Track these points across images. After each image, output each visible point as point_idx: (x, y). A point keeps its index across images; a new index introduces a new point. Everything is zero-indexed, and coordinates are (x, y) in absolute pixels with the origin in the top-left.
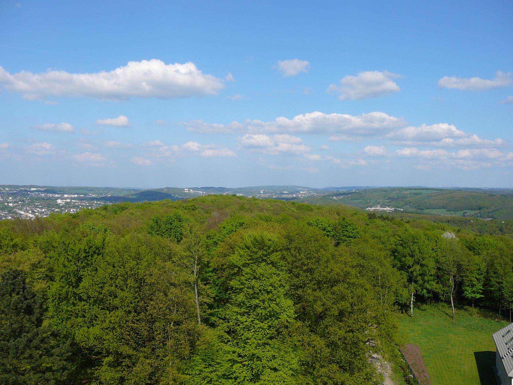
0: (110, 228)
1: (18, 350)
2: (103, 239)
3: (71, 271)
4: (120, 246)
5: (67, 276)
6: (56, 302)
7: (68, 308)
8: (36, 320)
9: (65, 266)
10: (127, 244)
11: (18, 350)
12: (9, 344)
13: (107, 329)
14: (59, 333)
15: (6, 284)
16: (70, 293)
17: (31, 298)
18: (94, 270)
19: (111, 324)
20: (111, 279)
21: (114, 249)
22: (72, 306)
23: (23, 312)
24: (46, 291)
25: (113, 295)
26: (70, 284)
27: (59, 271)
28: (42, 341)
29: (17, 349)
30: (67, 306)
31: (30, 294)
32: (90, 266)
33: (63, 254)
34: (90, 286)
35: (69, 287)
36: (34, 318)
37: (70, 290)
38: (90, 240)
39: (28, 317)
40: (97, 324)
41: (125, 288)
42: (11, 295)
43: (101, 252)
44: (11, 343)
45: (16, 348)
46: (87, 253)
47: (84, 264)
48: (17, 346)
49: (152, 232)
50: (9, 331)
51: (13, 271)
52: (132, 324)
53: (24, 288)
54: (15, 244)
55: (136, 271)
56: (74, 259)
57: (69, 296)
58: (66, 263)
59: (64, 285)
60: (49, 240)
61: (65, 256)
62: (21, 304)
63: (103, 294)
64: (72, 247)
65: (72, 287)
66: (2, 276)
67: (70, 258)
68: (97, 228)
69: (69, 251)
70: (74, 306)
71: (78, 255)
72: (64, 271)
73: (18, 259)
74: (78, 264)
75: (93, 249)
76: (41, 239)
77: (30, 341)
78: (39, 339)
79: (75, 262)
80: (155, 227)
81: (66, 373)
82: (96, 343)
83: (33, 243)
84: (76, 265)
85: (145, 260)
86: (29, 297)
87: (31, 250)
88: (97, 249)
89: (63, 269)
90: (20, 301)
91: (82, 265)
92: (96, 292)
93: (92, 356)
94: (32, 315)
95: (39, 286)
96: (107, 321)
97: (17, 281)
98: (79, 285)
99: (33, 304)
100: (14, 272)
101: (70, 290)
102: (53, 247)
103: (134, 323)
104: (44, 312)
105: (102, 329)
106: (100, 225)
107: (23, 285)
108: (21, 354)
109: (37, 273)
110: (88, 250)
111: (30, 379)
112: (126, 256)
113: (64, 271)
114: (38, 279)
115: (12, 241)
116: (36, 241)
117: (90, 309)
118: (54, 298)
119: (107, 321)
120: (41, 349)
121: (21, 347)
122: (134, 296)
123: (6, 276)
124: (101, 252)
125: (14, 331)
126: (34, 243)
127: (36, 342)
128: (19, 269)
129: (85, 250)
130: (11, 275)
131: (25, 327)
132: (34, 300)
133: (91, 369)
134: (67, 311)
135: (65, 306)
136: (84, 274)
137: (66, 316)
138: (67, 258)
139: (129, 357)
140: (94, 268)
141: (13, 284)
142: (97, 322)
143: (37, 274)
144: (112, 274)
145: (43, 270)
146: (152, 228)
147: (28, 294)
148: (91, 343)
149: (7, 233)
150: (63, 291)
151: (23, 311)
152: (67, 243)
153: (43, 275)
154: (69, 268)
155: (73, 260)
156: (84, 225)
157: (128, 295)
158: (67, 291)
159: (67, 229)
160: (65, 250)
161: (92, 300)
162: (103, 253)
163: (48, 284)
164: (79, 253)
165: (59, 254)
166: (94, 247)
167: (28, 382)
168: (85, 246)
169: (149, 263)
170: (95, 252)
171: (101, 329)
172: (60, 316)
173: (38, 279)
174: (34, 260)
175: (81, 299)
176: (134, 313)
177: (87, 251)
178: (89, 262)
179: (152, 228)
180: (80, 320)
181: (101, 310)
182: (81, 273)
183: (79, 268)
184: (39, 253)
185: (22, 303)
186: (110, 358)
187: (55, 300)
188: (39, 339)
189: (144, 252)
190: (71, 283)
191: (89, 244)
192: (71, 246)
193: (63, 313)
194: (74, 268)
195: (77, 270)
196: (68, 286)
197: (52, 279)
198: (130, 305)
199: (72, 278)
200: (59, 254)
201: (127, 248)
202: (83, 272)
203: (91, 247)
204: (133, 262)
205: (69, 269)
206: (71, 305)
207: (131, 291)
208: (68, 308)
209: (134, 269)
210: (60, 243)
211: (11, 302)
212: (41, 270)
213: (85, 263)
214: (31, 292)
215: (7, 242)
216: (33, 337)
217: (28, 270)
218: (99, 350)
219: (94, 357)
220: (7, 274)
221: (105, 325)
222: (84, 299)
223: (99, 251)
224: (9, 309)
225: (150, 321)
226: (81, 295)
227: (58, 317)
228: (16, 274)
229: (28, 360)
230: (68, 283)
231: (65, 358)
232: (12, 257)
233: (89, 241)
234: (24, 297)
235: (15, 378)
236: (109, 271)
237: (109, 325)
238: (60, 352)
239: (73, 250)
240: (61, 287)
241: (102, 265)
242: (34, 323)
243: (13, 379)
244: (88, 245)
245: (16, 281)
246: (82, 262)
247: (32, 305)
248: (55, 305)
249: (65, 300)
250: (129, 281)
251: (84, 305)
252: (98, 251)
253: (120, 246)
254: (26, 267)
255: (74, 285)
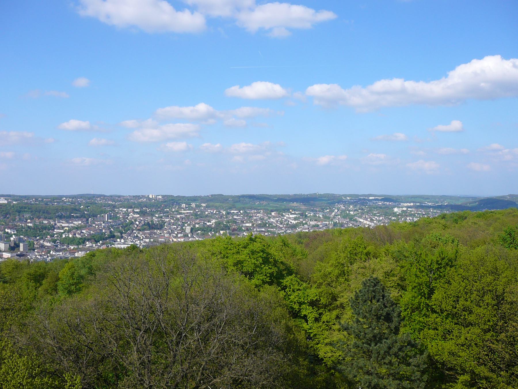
0: (458, 239)
1: (379, 354)
2: (455, 251)
3: (423, 282)
4: (475, 259)
5: (420, 287)
6: (408, 312)
7: (421, 319)
8: (395, 328)
9: (416, 276)
10: (482, 258)
11: (379, 354)
12: (371, 348)
13: (463, 346)
14: (416, 343)
15: (368, 291)
16: (422, 304)
17: (390, 306)
18: (446, 282)
19: (467, 342)
20: (466, 293)
21: (469, 262)
22: (424, 317)
23: (382, 319)
24: (399, 300)
25: (468, 310)
26: (423, 295)
27: (411, 281)
28: (400, 349)
29: (379, 353)
30: (419, 317)
31: (389, 302)
32: (443, 278)
33: (414, 265)
34: (443, 299)
35: (421, 298)
36: (393, 326)
37: (422, 301)
38: (442, 251)
39: (388, 324)
40: (452, 339)
41: (481, 304)
42: (371, 302)
43: (453, 264)
44: (373, 347)
45: (378, 353)
46: (439, 264)
47: (436, 275)
48: (378, 351)
49: (504, 245)
50: (371, 335)
51: (373, 279)
52: (491, 345)
53: (383, 296)
54: (368, 252)
55: (493, 287)
56: (426, 270)
57: (421, 308)
58: (418, 273)
59: (416, 295)
60: (400, 249)
61: (417, 266)
62: (381, 312)
63: (457, 308)
64: (425, 258)
65: (424, 298)
66: (364, 283)
67: (423, 269)
68: (444, 239)
69: (421, 262)
70: (426, 317)
71: (430, 266)
72: (416, 281)
73: (372, 266)
74: (430, 276)
75: (446, 260)
76: (393, 248)
77: (390, 348)
78: (398, 346)
79: (427, 273)
80: (508, 239)
81: (423, 385)
82: (452, 358)
83: (385, 252)
84: (428, 276)
85: (504, 275)
86: (388, 305)
87: (384, 258)
88: (450, 260)
89: (416, 279)
90: (381, 308)
91: (434, 277)
92: (449, 306)
93: (445, 371)
94: (391, 323)
95: (394, 294)
96: (463, 338)
97: (378, 289)
98: (432, 296)
99: (392, 312)
100: (375, 279)
101: (422, 301)
102: (405, 257)
103: (493, 343)
104: (401, 321)
105: (457, 345)
106: (447, 236)
107: (383, 293)
108: (381, 359)
109: (390, 281)
110: (440, 261)
111: (390, 385)
112: (482, 270)
113: (416, 281)
114: (391, 287)
115: (365, 249)
116: (387, 250)
117: (442, 322)
118: (407, 307)
119: (463, 338)
120: (400, 357)
121: (382, 352)
122: (492, 314)
123: (367, 282)
124: (453, 264)
125: (374, 336)
126: (386, 251)
127: (395, 349)
128: (374, 276)
129: (437, 261)
130: (372, 282)
131: (384, 333)
132: (393, 308)
133: (445, 384)
134: (420, 321)
135: (417, 316)
136: (436, 287)
137: (418, 326)
138: (419, 269)
139: (486, 378)
140: (446, 280)
141: (374, 291)
142: (451, 337)
143: (390, 282)
144: (467, 288)
145: (395, 278)
146: (504, 240)
147: (388, 302)
148: (445, 357)
149: (361, 241)
150: (416, 301)
151: (383, 317)
152: (419, 253)
153: (395, 283)
154: (421, 278)
155: (426, 271)
156: (431, 235)
157: (485, 312)
158: (419, 302)
159: (417, 239)
160: (417, 260)
161: (445, 314)
162: (455, 266)
163: (400, 293)
164: (431, 264)
165: (410, 264)
166: (447, 259)
167: (388, 387)
168: (437, 257)
169: (509, 280)
170: (447, 264)
171: (456, 345)
172: (412, 326)
173: (391, 287)
174: (388, 269)
175: (434, 311)
176: (492, 333)
177: (440, 262)
178: (441, 274)
179: (504, 240)
180: (432, 332)
181: (455, 324)
182: (433, 284)
183: (432, 279)
184: (391, 261)
185: (382, 310)
186: (466, 377)
187: (407, 309)
188: (398, 346)
189: (502, 267)
190: (423, 294)
191: (441, 255)
192: (423, 257)
193: (415, 323)
194: (425, 279)
195: (430, 281)
196: (420, 297)
197: (403, 288)
198: (489, 323)
199: (424, 289)
200: (410, 264)
201: (482, 261)
202: (436, 283)
203: (443, 259)
204: (491, 277)
205: (421, 280)
206: (423, 317)
207: (489, 308)
208: (421, 319)
209: (491, 284)
210: (412, 253)
211: (372, 308)
212: (393, 278)
213: (438, 275)
214: (390, 300)
215: (361, 250)
216: (392, 344)
217: (381, 278)
218: (452, 366)
219: (447, 372)
220: (368, 282)
221: (460, 342)
222: (437, 311)
223: (452, 264)
224: (370, 314)
225: (512, 344)
226: (434, 307)
227: (410, 327)
228: (376, 282)
229: (388, 366)
230: (421, 294)
231: (422, 369)
232: (366, 264)
233: (441, 252)
234: (384, 305)
235: (377, 381)
236: (463, 284)
237: (465, 341)
238: (418, 362)
239: (426, 260)
240: (413, 297)
241: (456, 278)
242: (392, 330)
243: (375, 381)
244: (440, 256)
245: (376, 289)
246: (434, 274)
247: (391, 313)
248: (408, 314)
249: (416, 311)
250: (486, 298)
251: (437, 318)
252: (451, 263)
253: (475, 259)
254: (380, 275)
255: (426, 296)
